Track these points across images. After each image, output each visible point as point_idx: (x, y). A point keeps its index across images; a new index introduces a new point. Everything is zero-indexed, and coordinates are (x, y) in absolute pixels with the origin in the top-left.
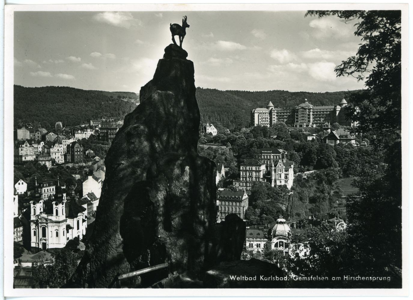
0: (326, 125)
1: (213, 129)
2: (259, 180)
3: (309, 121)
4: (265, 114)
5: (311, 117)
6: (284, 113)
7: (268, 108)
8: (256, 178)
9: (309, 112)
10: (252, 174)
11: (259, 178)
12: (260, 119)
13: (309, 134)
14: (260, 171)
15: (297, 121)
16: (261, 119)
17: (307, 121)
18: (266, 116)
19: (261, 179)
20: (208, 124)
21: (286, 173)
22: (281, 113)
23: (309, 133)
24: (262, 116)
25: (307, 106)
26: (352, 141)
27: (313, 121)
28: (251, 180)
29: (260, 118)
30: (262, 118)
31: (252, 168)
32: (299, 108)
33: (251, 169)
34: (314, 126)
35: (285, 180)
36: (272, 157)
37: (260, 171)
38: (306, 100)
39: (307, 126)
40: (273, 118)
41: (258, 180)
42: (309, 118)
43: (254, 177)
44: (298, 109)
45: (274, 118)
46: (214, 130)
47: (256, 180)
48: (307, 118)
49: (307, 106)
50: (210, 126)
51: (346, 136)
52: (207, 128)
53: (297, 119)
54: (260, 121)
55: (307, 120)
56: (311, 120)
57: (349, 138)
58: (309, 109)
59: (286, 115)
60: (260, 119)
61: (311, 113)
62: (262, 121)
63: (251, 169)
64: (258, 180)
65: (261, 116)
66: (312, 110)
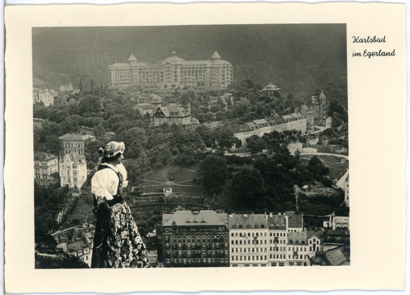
0: (155, 99)
1: (48, 96)
2: (46, 177)
3: (176, 80)
4: (125, 70)
5: (179, 74)
6: (148, 69)
7: (129, 62)
8: (43, 175)
9: (176, 69)
10: (39, 171)
11: (46, 175)
12: (118, 77)
13: (147, 107)
14: (48, 167)
15: (162, 80)
16: (120, 78)
17: (173, 80)
18: (126, 73)
19: (49, 176)
20: (40, 91)
21: (75, 169)
22: (144, 69)
23: (148, 104)
24: (121, 73)
25: (174, 61)
26: (183, 119)
27: (182, 79)
28: (38, 178)
29: (118, 76)
30: (121, 77)
31: (38, 164)
32: (165, 63)
33: (37, 165)
34: (182, 86)
35: (74, 179)
36: (74, 146)
37: (48, 167)
38: (174, 52)
39: (174, 86)
40: (135, 75)
41: (45, 178)
42: (176, 76)
43: (41, 174)
44: (163, 65)
45: (136, 75)
46: (49, 97)
47: (44, 177)
48: (173, 77)
49: (174, 61)
50: (44, 92)
51: (177, 113)
52: (39, 95)
53: (162, 77)
54: (118, 79)
55: (174, 78)
56: (179, 78)
57: (180, 116)
58: (176, 65)
59: (151, 72)
60: (118, 77)
61: (179, 70)
62: (121, 80)
63: (37, 165)
64: (45, 178)
65: (120, 74)
66: (179, 67)
